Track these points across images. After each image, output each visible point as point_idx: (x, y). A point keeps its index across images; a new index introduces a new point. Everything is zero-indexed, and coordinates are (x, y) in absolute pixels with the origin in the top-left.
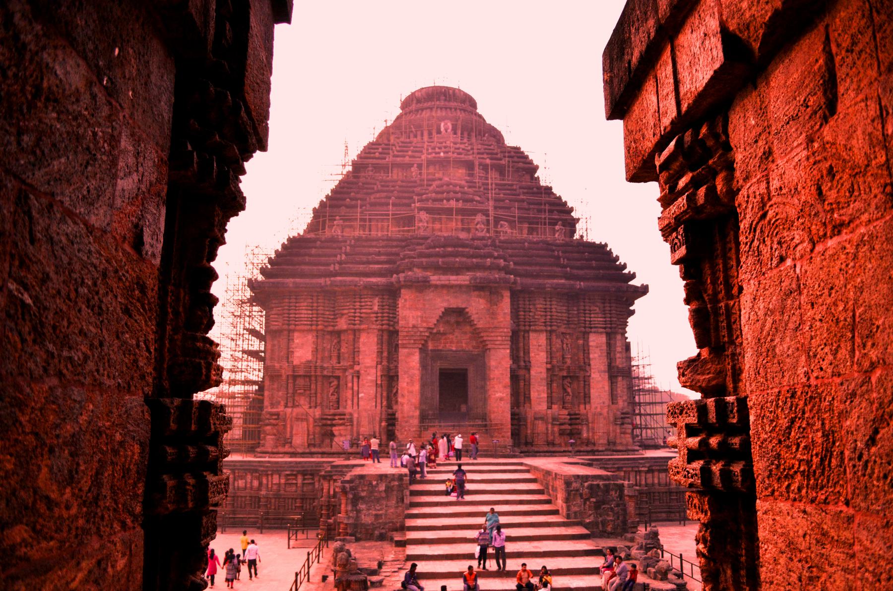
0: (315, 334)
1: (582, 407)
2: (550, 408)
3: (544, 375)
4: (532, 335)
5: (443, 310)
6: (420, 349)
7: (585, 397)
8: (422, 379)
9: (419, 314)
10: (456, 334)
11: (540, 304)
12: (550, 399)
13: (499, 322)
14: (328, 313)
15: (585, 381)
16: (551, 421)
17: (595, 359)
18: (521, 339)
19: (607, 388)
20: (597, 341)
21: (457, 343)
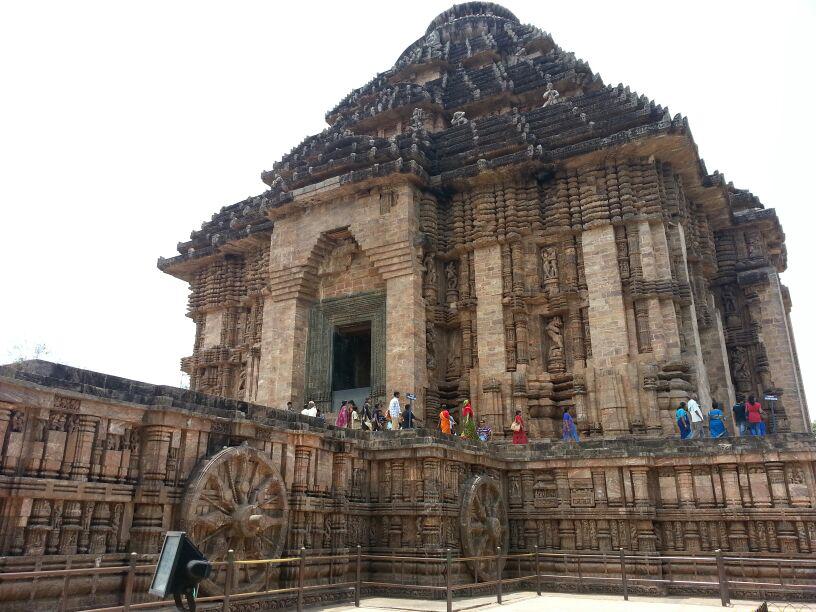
0: (225, 311)
1: (578, 364)
2: (511, 369)
3: (499, 316)
4: (478, 256)
5: (318, 236)
6: (299, 299)
7: (585, 347)
8: (309, 343)
9: (292, 249)
10: (352, 271)
11: (483, 204)
12: (514, 355)
13: (392, 235)
14: (238, 284)
15: (582, 318)
16: (507, 390)
17: (596, 274)
18: (464, 267)
19: (622, 323)
20: (599, 245)
21: (355, 284)
